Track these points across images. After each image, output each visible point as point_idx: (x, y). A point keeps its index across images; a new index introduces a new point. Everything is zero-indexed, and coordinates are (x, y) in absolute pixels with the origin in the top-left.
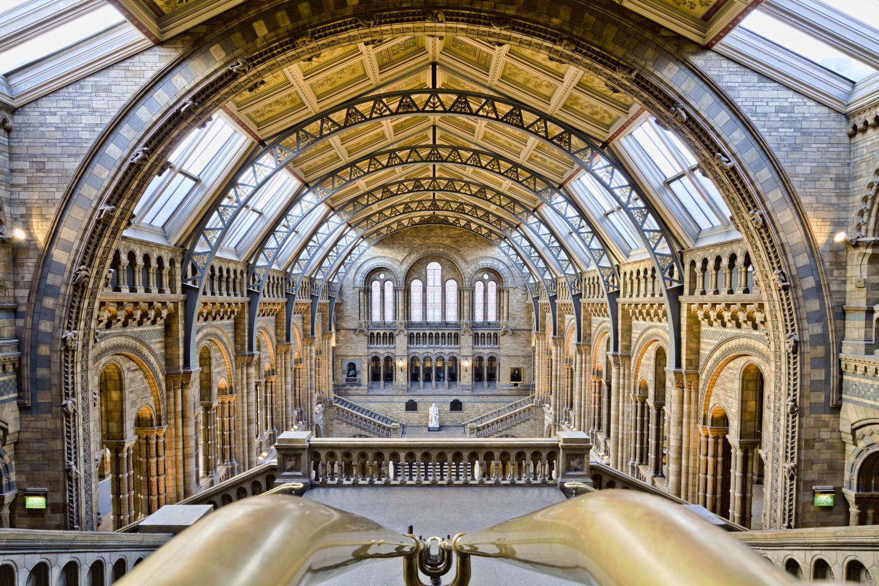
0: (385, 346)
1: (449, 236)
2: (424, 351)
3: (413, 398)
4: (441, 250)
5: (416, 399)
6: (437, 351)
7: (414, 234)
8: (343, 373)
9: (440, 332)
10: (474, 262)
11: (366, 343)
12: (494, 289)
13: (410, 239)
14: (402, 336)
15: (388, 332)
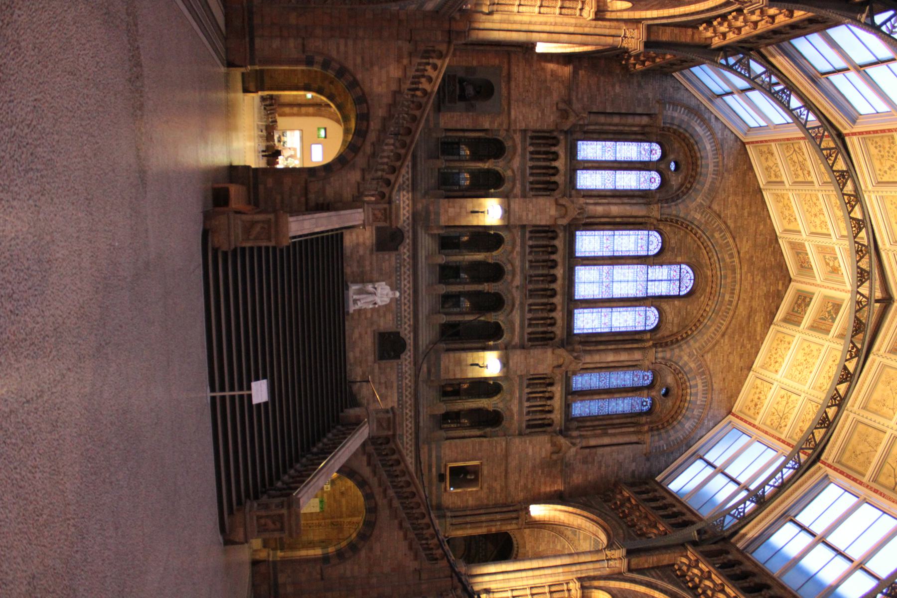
0: (528, 171)
1: (751, 312)
2: (517, 263)
3: (408, 240)
4: (727, 297)
5: (405, 251)
6: (517, 295)
7: (760, 239)
8: (470, 70)
9: (558, 300)
10: (700, 366)
11: (538, 126)
12: (637, 408)
13: (752, 229)
14: (553, 212)
15: (560, 179)
